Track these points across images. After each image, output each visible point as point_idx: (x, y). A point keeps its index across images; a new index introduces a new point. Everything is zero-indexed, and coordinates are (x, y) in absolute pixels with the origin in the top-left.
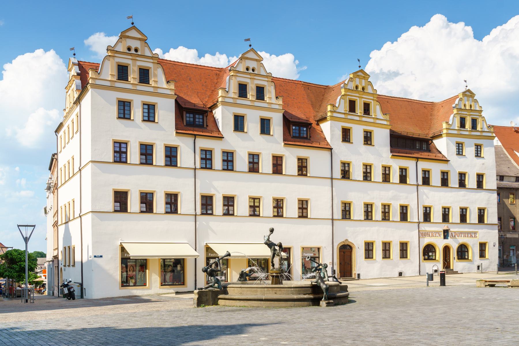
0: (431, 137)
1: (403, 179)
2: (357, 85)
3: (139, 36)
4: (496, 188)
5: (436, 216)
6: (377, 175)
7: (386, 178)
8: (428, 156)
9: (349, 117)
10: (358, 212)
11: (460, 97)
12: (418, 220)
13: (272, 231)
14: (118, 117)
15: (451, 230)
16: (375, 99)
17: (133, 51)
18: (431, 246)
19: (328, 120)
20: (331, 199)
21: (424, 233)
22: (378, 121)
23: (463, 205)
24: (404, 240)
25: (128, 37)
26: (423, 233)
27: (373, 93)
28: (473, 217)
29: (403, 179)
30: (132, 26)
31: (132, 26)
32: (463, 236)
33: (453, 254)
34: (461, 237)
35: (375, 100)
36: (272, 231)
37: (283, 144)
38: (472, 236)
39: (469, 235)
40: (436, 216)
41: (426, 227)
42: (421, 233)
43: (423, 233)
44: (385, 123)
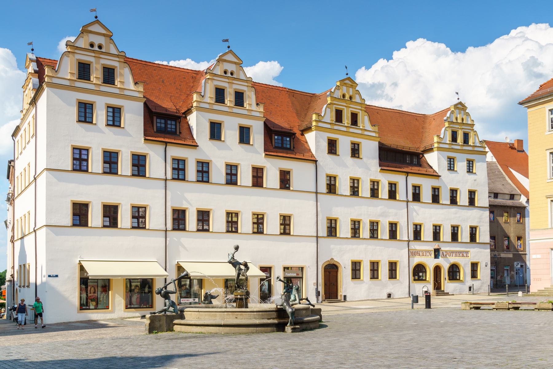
0: (421, 151)
1: (392, 195)
2: (344, 93)
3: (104, 32)
4: (488, 206)
5: (427, 234)
6: (365, 190)
7: (374, 193)
8: (419, 170)
9: (336, 127)
10: (344, 229)
11: (451, 110)
13: (237, 248)
14: (78, 121)
15: (443, 249)
16: (363, 109)
17: (96, 48)
18: (421, 266)
19: (313, 129)
20: (316, 214)
21: (414, 252)
22: (366, 133)
23: (455, 223)
24: (393, 259)
25: (91, 32)
26: (413, 252)
27: (361, 102)
28: (464, 236)
29: (392, 195)
30: (95, 19)
31: (95, 19)
32: (454, 255)
33: (444, 274)
34: (453, 256)
35: (363, 110)
36: (237, 248)
37: (264, 154)
38: (464, 256)
39: (461, 255)
40: (427, 234)
41: (416, 246)
42: (411, 252)
43: (413, 252)
44: (374, 134)
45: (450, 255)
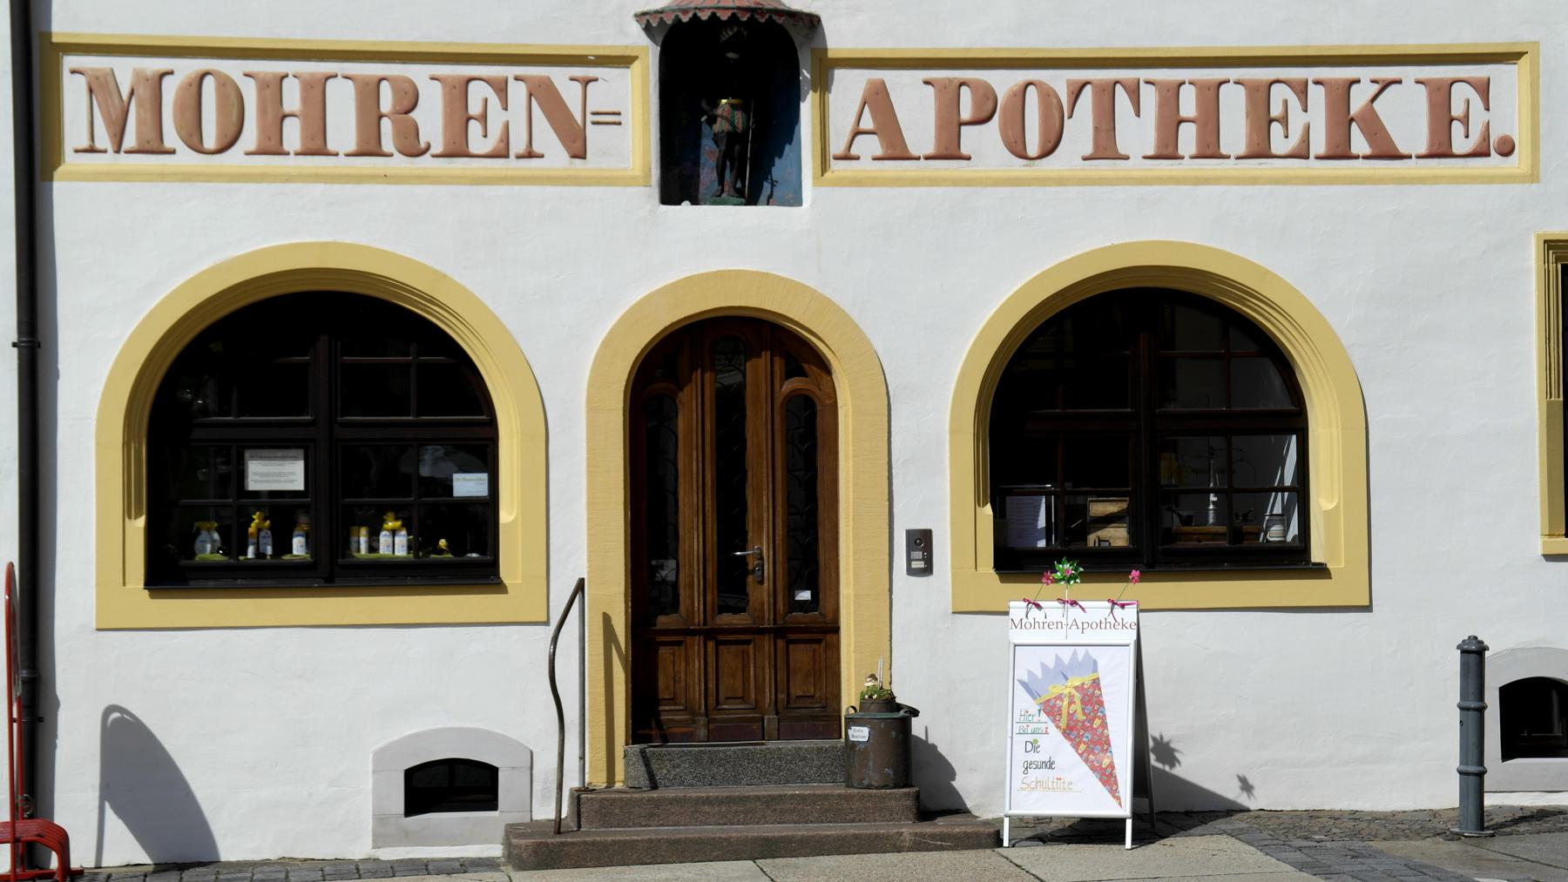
34: (1105, 147)
39: (1315, 118)
42: (99, 87)
45: (1033, 145)
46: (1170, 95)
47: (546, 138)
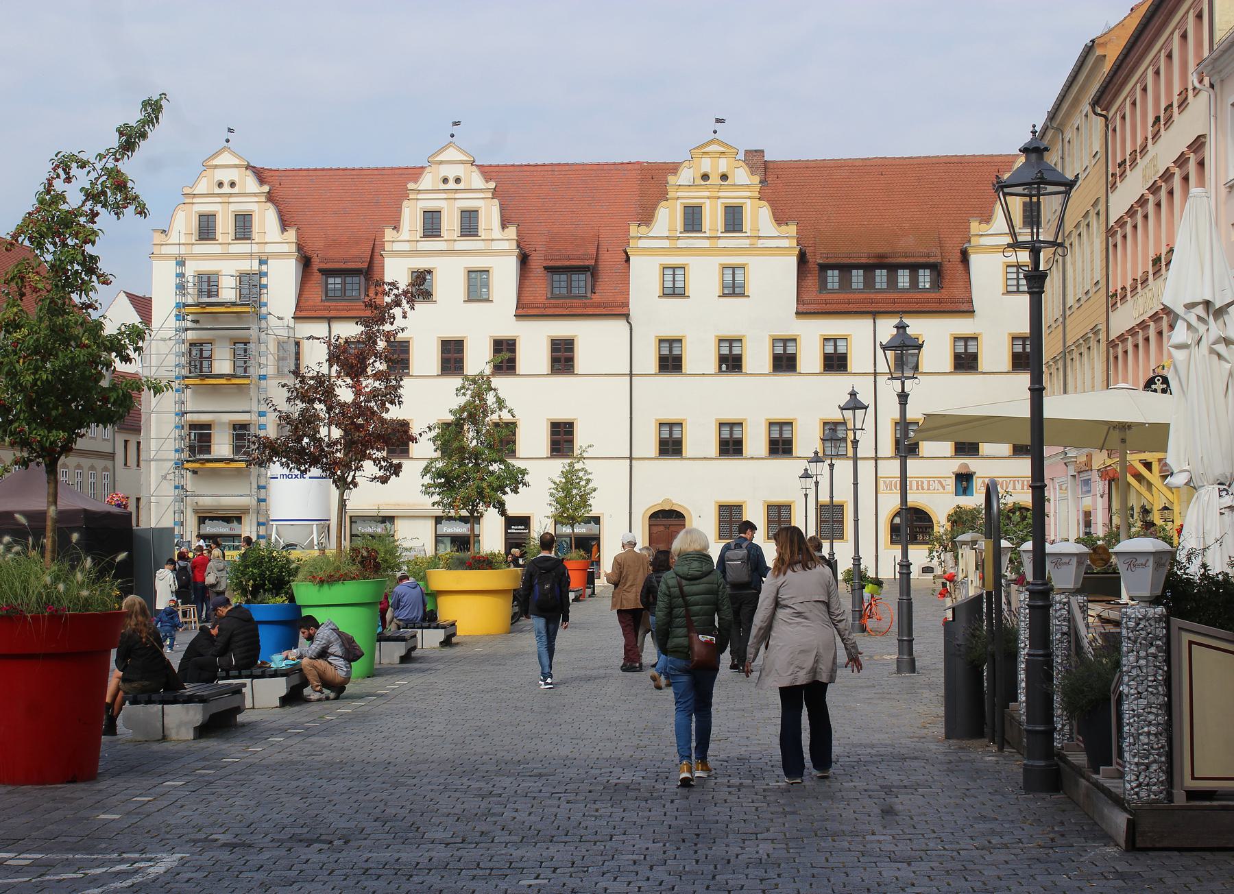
6: (757, 357)
7: (784, 362)
12: (876, 452)
22: (760, 243)
35: (754, 198)
42: (885, 482)
46: (1023, 482)
47: (940, 488)
